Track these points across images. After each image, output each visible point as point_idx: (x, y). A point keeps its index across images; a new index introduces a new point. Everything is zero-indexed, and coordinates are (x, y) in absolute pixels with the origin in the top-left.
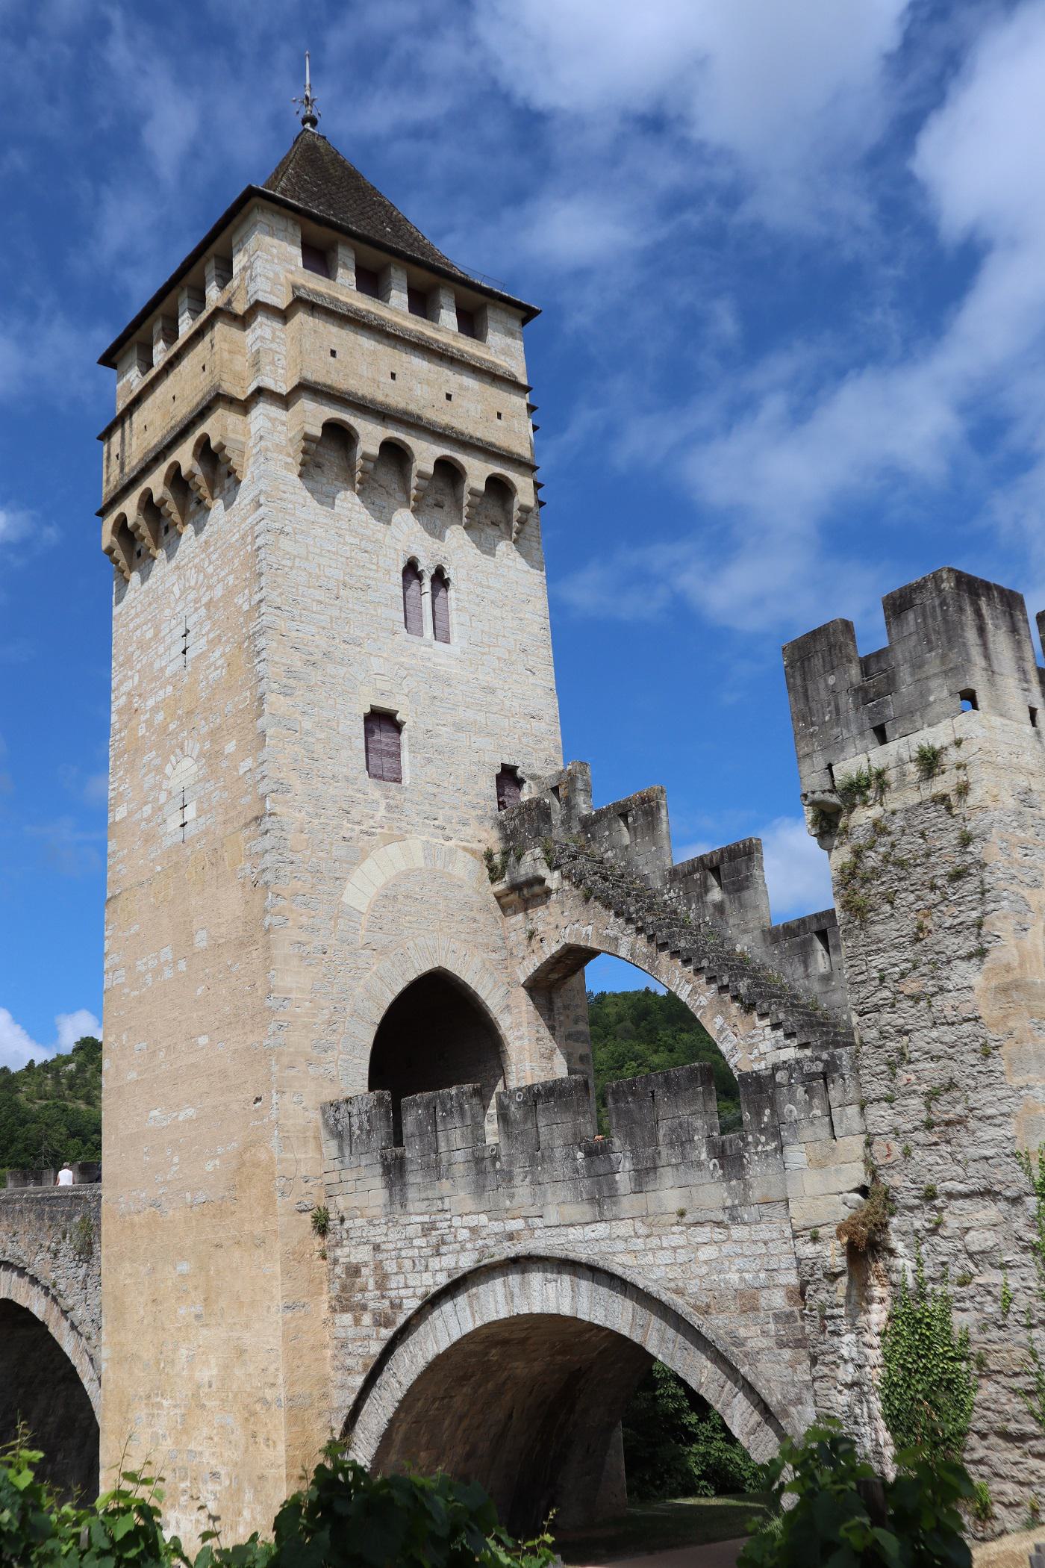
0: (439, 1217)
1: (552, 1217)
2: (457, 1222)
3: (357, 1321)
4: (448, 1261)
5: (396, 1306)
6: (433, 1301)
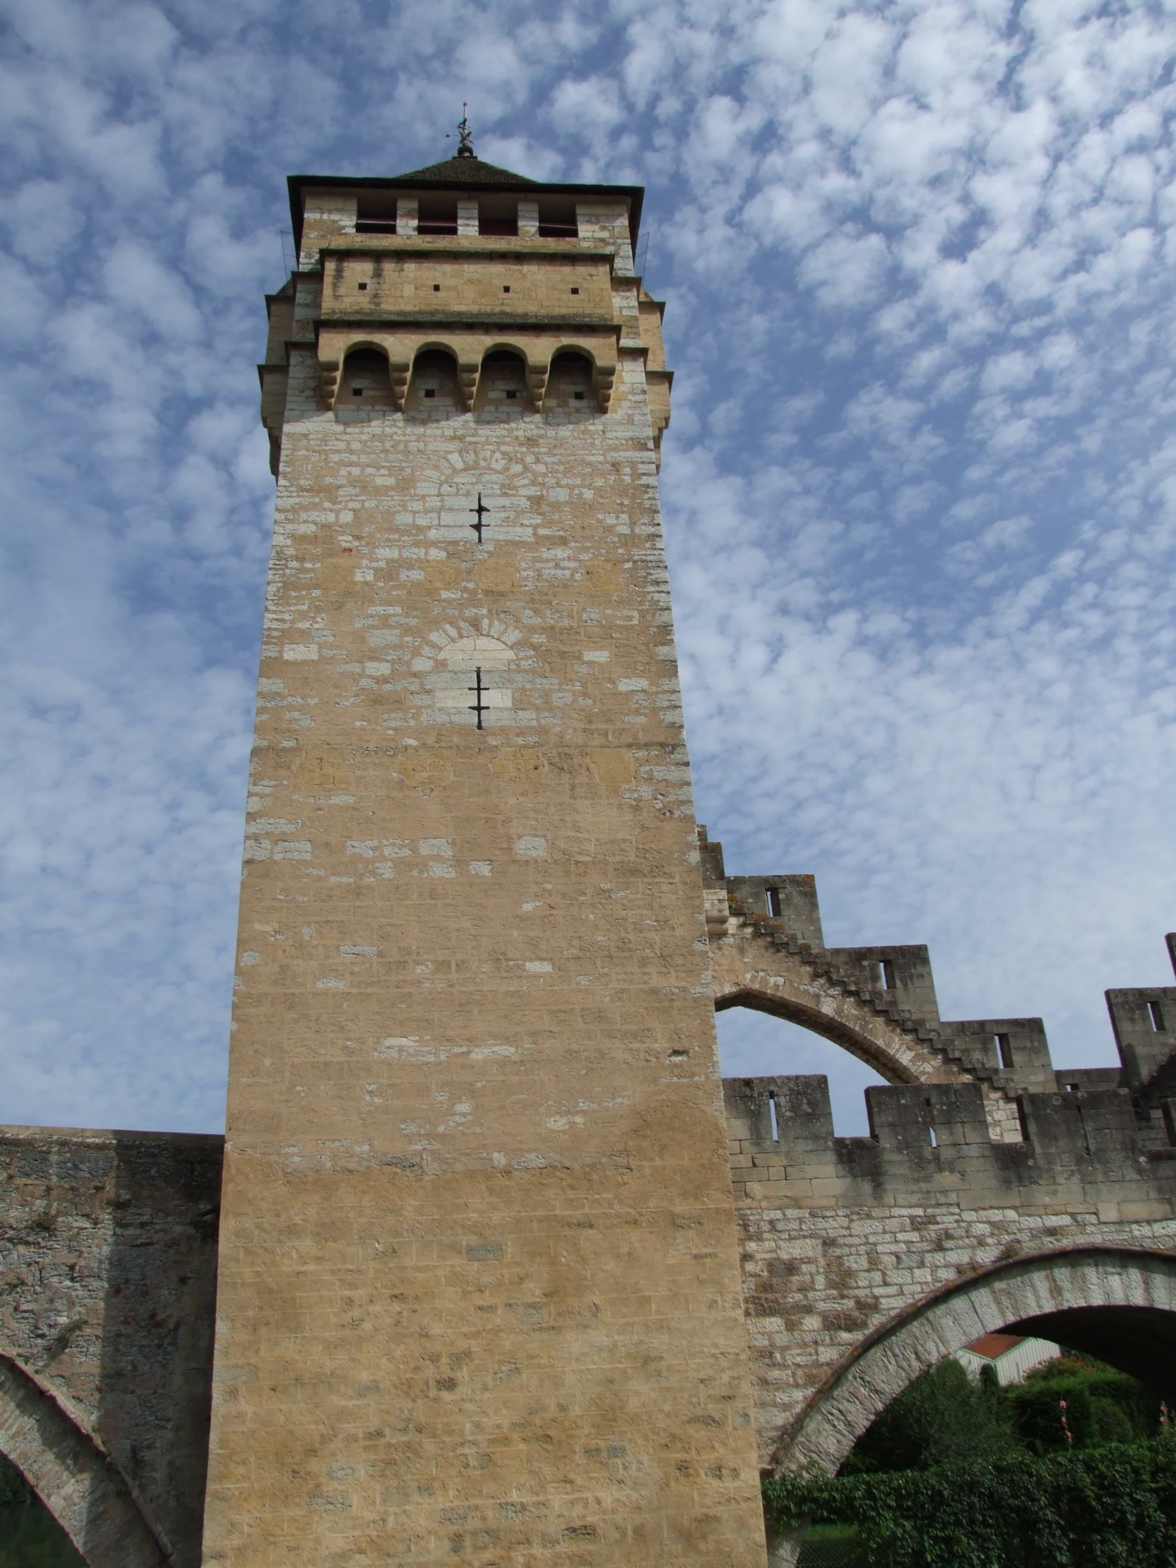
0: (938, 1211)
1: (1110, 1213)
2: (968, 1216)
3: (791, 1326)
4: (961, 1257)
5: (869, 1306)
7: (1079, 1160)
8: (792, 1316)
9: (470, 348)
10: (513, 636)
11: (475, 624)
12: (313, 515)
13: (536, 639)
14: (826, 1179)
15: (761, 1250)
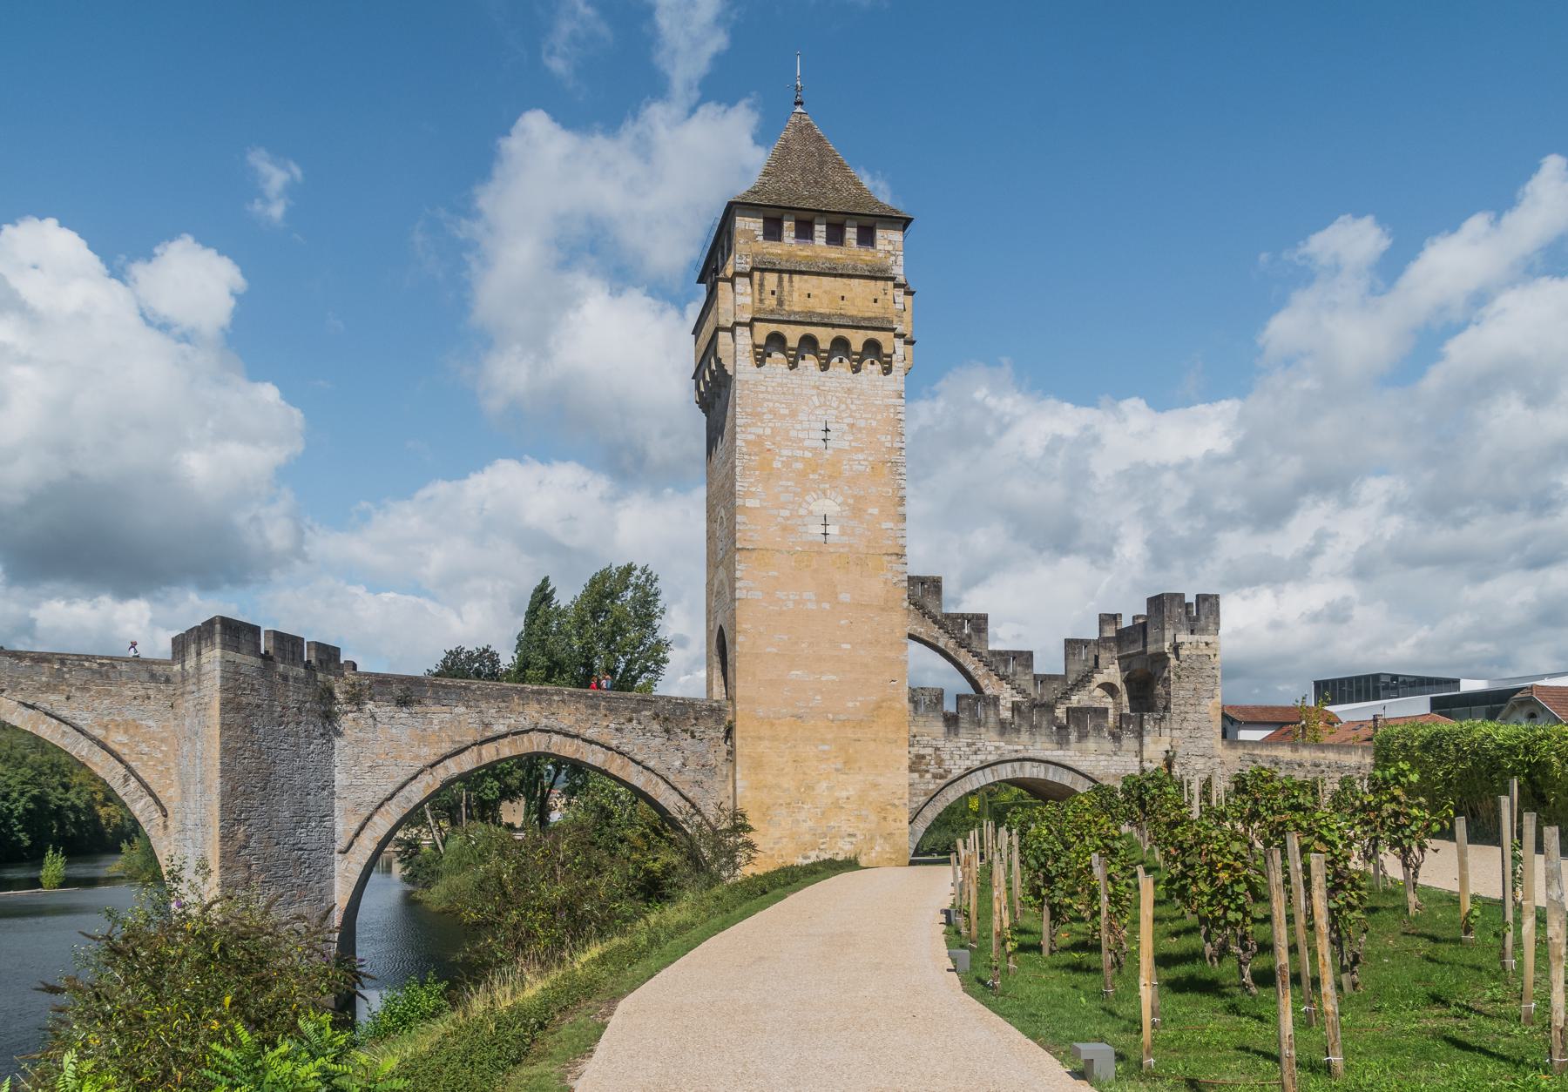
6: (970, 771)
7: (1032, 726)
8: (922, 773)
9: (825, 337)
10: (840, 499)
11: (824, 492)
12: (753, 430)
13: (851, 501)
14: (939, 727)
15: (914, 750)
